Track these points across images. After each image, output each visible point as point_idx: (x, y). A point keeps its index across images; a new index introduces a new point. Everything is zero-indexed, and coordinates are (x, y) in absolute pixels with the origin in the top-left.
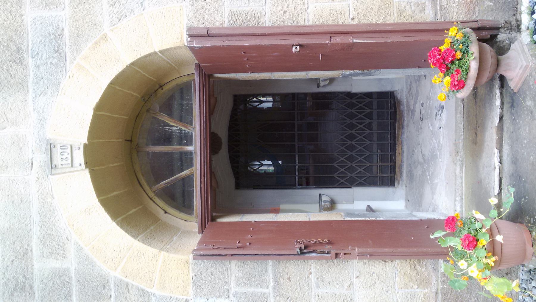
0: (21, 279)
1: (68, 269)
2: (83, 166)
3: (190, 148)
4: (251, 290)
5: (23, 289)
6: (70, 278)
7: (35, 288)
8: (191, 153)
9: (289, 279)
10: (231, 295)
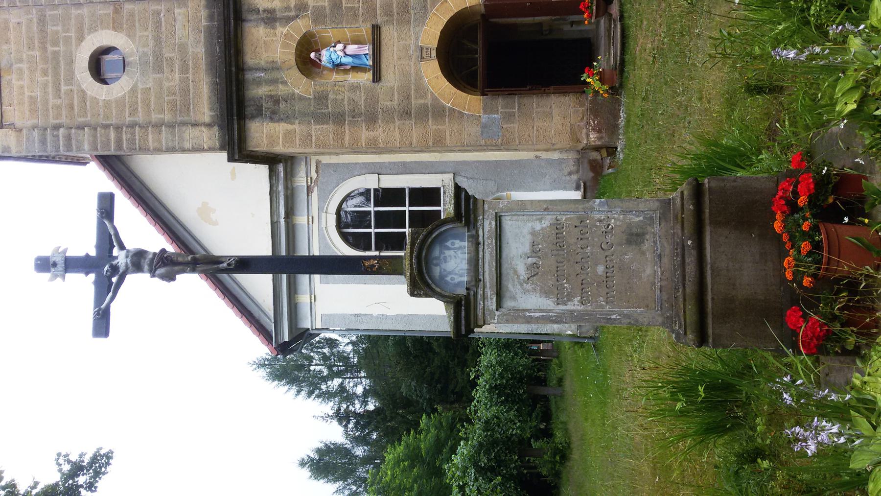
1: (427, 104)
3: (477, 56)
4: (507, 110)
5: (407, 113)
6: (428, 107)
7: (412, 112)
8: (477, 58)
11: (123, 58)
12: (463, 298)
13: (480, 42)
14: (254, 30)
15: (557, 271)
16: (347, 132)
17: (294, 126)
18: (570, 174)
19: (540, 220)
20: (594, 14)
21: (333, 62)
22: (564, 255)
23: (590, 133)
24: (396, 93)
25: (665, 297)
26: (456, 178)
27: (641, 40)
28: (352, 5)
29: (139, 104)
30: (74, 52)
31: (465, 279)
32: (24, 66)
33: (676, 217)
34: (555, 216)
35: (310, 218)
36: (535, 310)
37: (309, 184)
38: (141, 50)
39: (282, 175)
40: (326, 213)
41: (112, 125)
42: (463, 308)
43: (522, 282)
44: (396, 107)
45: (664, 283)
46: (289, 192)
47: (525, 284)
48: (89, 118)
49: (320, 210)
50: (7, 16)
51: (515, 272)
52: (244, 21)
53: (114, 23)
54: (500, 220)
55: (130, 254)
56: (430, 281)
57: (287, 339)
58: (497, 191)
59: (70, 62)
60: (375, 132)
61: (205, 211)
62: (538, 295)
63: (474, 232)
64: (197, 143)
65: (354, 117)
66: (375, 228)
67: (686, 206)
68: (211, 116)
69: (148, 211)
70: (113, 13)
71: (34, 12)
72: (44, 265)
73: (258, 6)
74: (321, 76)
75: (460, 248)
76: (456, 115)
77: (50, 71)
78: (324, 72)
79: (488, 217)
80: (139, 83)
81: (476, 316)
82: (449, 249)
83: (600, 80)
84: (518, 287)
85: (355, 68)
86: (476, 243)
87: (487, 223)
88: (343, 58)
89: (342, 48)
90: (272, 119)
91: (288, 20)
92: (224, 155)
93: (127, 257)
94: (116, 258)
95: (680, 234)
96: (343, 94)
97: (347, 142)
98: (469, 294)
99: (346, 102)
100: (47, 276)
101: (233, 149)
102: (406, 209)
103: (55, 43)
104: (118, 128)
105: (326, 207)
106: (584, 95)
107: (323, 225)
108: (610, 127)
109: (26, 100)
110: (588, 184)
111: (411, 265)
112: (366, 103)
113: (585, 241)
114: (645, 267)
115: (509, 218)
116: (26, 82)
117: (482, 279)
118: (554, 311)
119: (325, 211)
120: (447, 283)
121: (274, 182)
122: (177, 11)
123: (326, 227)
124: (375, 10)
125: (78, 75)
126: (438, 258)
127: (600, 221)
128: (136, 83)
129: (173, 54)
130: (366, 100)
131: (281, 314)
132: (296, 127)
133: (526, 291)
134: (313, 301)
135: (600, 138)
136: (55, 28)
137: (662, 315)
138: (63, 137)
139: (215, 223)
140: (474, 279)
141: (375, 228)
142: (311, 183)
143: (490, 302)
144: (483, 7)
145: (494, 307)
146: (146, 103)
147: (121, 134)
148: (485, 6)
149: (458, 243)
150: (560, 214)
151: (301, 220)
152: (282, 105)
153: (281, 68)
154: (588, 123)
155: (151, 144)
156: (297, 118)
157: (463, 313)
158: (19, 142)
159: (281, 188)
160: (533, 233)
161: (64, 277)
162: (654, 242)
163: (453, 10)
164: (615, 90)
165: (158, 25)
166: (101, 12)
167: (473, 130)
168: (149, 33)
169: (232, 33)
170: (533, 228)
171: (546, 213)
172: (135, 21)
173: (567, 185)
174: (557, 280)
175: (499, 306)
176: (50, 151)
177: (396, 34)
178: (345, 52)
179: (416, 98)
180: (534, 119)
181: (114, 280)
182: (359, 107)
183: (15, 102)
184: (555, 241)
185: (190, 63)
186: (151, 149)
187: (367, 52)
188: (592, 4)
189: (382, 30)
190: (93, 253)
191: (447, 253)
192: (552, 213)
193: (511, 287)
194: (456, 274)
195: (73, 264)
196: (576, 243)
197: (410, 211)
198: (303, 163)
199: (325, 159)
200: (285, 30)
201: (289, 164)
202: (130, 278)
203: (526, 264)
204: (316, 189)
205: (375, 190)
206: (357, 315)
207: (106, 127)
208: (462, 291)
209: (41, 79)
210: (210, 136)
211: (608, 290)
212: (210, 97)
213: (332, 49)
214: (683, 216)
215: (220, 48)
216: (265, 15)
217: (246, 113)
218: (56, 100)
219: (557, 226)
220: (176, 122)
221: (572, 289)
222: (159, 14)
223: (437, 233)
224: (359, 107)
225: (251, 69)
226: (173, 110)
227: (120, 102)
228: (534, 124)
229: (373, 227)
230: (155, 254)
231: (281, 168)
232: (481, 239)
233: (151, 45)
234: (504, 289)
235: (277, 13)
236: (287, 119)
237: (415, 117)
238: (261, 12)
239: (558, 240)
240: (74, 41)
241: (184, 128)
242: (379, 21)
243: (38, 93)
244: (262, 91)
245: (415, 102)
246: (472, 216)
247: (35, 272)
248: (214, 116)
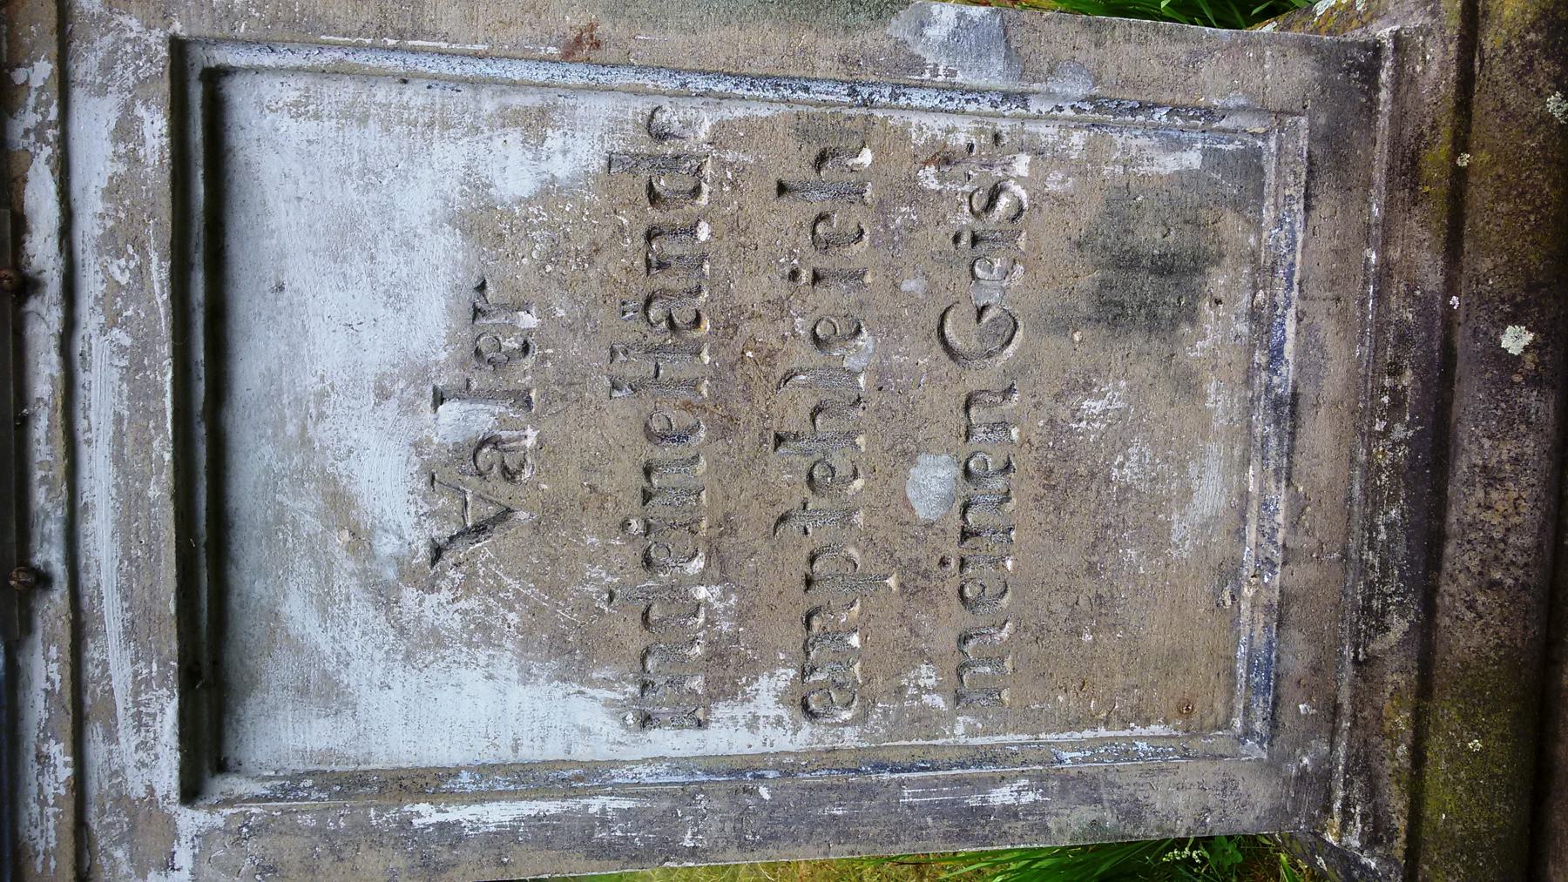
15: (647, 496)
19: (535, 124)
22: (694, 385)
25: (1298, 657)
33: (1407, 168)
34: (642, 106)
36: (484, 770)
43: (390, 573)
45: (1303, 575)
47: (410, 595)
51: (339, 503)
54: (216, 109)
62: (507, 663)
79: (107, 68)
84: (361, 610)
95: (1433, 280)
113: (830, 297)
114: (1193, 470)
115: (290, 91)
117: (59, 570)
118: (620, 777)
127: (945, 159)
137: (1273, 766)
143: (128, 739)
145: (167, 776)
150: (682, 93)
162: (1254, 315)
170: (477, 185)
171: (576, 75)
174: (648, 562)
184: (641, 286)
192: (625, 77)
196: (780, 307)
203: (417, 446)
211: (965, 619)
221: (741, 616)
234: (247, 627)
239: (660, 281)
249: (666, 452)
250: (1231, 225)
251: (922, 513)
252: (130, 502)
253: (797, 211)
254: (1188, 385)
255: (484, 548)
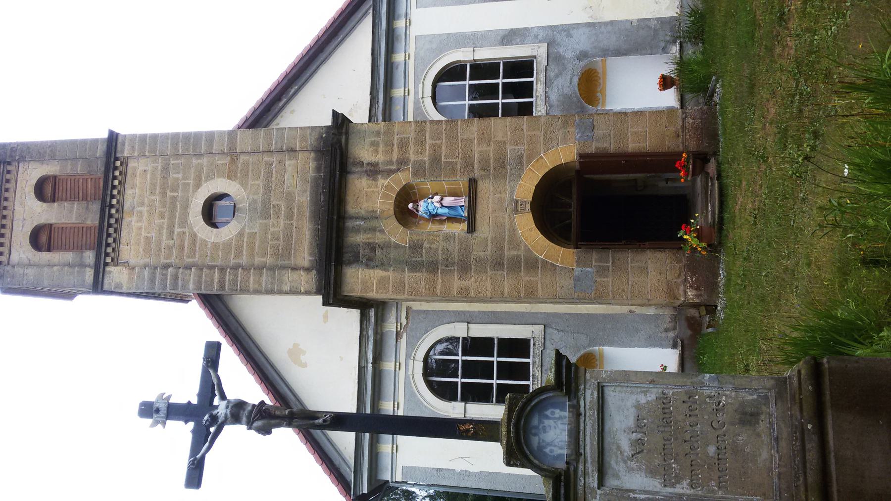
0: (499, 259)
1: (520, 255)
2: (530, 211)
3: (571, 210)
4: (601, 264)
5: (499, 264)
7: (505, 263)
9: (619, 260)
10: (593, 266)
11: (235, 204)
12: (563, 472)
13: (574, 197)
14: (357, 182)
15: (664, 449)
16: (440, 280)
17: (389, 273)
18: (666, 330)
19: (645, 393)
20: (691, 173)
21: (430, 213)
22: (671, 432)
23: (688, 290)
24: (490, 244)
26: (546, 330)
27: (741, 200)
28: (451, 160)
29: (245, 248)
30: (190, 199)
31: (565, 452)
32: (145, 209)
33: (793, 397)
34: (661, 390)
35: (398, 364)
36: (640, 491)
37: (399, 329)
38: (251, 197)
39: (373, 321)
40: (414, 360)
41: (217, 266)
42: (562, 483)
43: (626, 459)
44: (489, 258)
45: (783, 470)
46: (379, 337)
47: (629, 462)
48: (197, 259)
49: (408, 356)
50: (136, 164)
51: (619, 448)
52: (349, 173)
53: (229, 171)
54: (603, 390)
55: (231, 405)
56: (527, 452)
57: (365, 491)
58: (588, 346)
59: (186, 207)
60: (467, 282)
61: (295, 353)
62: (643, 474)
63: (575, 402)
64: (295, 287)
65: (447, 266)
66: (462, 378)
67: (804, 386)
68: (310, 260)
69: (241, 350)
70: (230, 163)
71: (160, 161)
72: (148, 410)
73: (363, 160)
74: (416, 224)
75: (560, 418)
76: (549, 267)
77: (167, 214)
78: (420, 222)
79: (590, 386)
80: (247, 227)
81: (576, 493)
82: (547, 417)
83: (697, 237)
84: (622, 464)
85: (450, 219)
86: (577, 414)
87: (588, 393)
88: (440, 209)
89: (439, 200)
90: (367, 266)
91: (390, 172)
92: (320, 298)
93: (227, 408)
94: (217, 407)
95: (799, 417)
96: (438, 244)
97: (439, 291)
98: (568, 468)
99: (440, 252)
100: (150, 421)
101: (328, 294)
102: (494, 359)
103: (174, 190)
104: (222, 270)
105: (413, 354)
106: (681, 251)
107: (410, 372)
108: (709, 284)
109: (142, 240)
110: (686, 342)
111: (508, 432)
112: (459, 253)
113: (692, 419)
114: (761, 450)
115: (612, 389)
116: (144, 224)
117: (583, 453)
118: (661, 494)
119: (412, 358)
120: (545, 454)
121: (365, 326)
122: (288, 163)
123: (413, 375)
124: (472, 165)
125: (191, 219)
126: (537, 428)
127: (710, 397)
128: (244, 228)
129: (281, 202)
130: (460, 249)
131: (362, 464)
132: (391, 274)
133: (630, 470)
134: (395, 451)
135: (698, 296)
136: (176, 176)
138: (171, 276)
139: (304, 365)
140: (574, 453)
141: (462, 378)
142: (401, 329)
144: (577, 164)
145: (596, 485)
146: (251, 246)
147: (225, 275)
148: (580, 162)
149: (558, 413)
150: (667, 388)
151: (389, 366)
152: (379, 253)
153: (380, 218)
154: (686, 280)
155: (252, 286)
156: (391, 266)
157: (562, 491)
158: (130, 279)
159: (371, 333)
160: (638, 406)
161: (164, 424)
162: (770, 423)
163: (547, 166)
164: (714, 247)
165: (269, 174)
166: (219, 162)
167: (565, 283)
168: (260, 183)
169: (337, 185)
172: (248, 172)
173: (664, 343)
174: (665, 460)
175: (601, 484)
176: (157, 289)
177: (491, 188)
178: (441, 204)
179: (509, 249)
180: (628, 274)
181: (212, 430)
182: (453, 256)
183: (132, 241)
184: (662, 417)
185: (295, 211)
186: (251, 290)
187: (464, 204)
188: (688, 163)
189: (478, 184)
190: (195, 401)
191: (547, 422)
192: (658, 386)
193: (614, 463)
194: (555, 446)
195: (175, 411)
197: (498, 362)
198: (394, 309)
199: (416, 306)
200: (386, 182)
201: (380, 310)
202: (227, 429)
203: (630, 439)
204: (405, 335)
205: (464, 339)
206: (439, 470)
207: (211, 268)
208: (561, 465)
209: (158, 221)
210: (307, 280)
211: (720, 474)
212: (311, 243)
213: (429, 201)
214: (801, 397)
215: (324, 198)
216: (369, 168)
217: (343, 259)
218: (168, 241)
219: (664, 400)
220: (277, 266)
222: (271, 165)
223: (536, 401)
224: (453, 256)
225: (351, 218)
226: (275, 254)
227: (227, 245)
228: (628, 279)
229: (460, 377)
230: (254, 406)
231: (372, 313)
232: (582, 409)
233: (261, 192)
235: (380, 166)
236: (382, 266)
237: (508, 268)
238: (365, 165)
239: (666, 416)
240: (191, 187)
241: (283, 272)
242: (476, 174)
243: (154, 234)
244: (360, 239)
245: (508, 253)
246: (573, 384)
247: (138, 417)
248: (313, 260)
249: (668, 442)
250: (764, 408)
251: (710, 455)
252: (592, 444)
253: (686, 405)
254: (759, 435)
255: (639, 456)
